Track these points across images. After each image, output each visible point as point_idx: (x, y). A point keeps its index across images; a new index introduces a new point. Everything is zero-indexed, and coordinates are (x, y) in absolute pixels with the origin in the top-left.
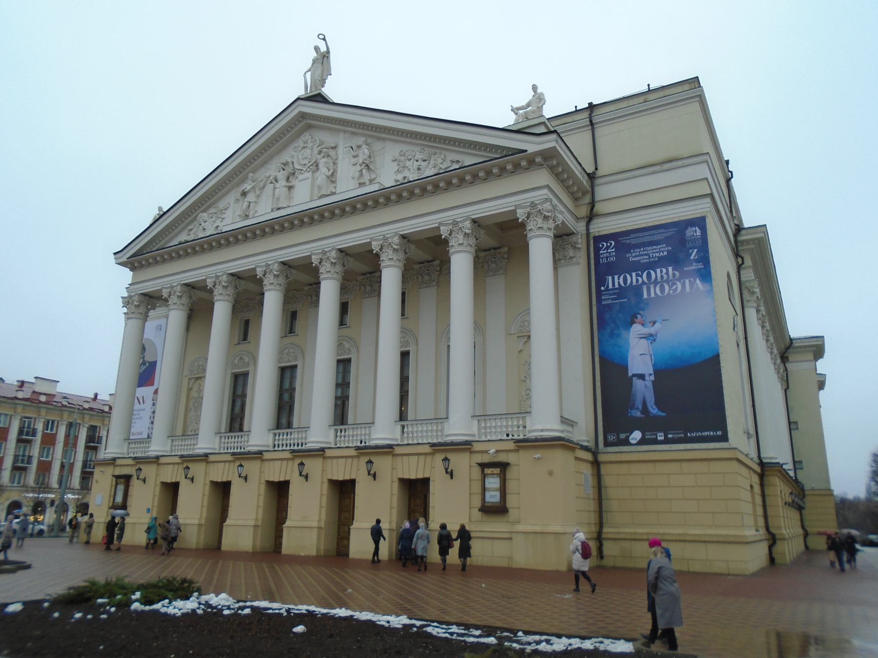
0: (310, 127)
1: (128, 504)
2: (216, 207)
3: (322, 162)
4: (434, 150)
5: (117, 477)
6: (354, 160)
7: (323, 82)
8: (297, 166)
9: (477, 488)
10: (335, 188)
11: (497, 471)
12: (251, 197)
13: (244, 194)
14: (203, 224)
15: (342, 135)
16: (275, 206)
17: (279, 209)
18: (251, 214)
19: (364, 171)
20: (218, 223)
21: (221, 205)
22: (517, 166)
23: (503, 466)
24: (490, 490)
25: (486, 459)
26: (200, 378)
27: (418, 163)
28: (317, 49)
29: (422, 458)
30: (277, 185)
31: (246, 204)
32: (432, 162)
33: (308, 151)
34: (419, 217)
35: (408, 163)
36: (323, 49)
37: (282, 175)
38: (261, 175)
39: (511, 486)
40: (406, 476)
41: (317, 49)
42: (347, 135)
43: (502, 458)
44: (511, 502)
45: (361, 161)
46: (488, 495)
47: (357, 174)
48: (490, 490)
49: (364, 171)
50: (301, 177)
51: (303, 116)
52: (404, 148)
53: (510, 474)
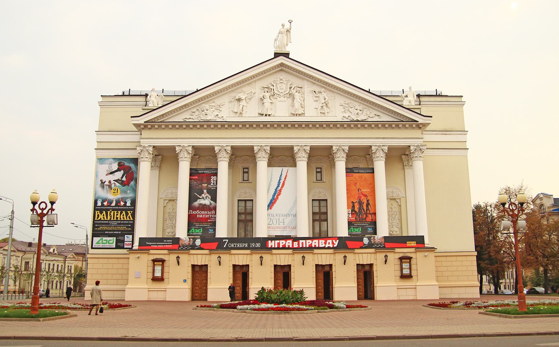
0: (281, 70)
1: (164, 277)
2: (214, 102)
3: (297, 95)
4: (366, 107)
5: (154, 261)
6: (316, 99)
7: (287, 45)
8: (275, 92)
9: (398, 267)
10: (304, 111)
11: (409, 261)
12: (243, 103)
13: (239, 100)
14: (206, 111)
15: (306, 82)
16: (265, 113)
17: (266, 115)
18: (244, 112)
19: (325, 107)
20: (216, 113)
21: (218, 101)
22: (411, 126)
23: (410, 258)
24: (405, 269)
25: (401, 255)
26: (174, 200)
27: (358, 111)
28: (283, 25)
29: (328, 255)
30: (265, 101)
31: (241, 106)
32: (364, 112)
33: (284, 86)
34: (360, 138)
35: (350, 109)
36: (287, 26)
37: (267, 95)
38: (248, 89)
39: (413, 267)
40: (361, 263)
41: (283, 25)
42: (309, 83)
43: (409, 255)
44: (413, 273)
45: (323, 101)
46: (404, 271)
47: (320, 108)
48: (405, 269)
49: (325, 107)
50: (278, 98)
51: (282, 65)
52: (348, 101)
53: (413, 261)
